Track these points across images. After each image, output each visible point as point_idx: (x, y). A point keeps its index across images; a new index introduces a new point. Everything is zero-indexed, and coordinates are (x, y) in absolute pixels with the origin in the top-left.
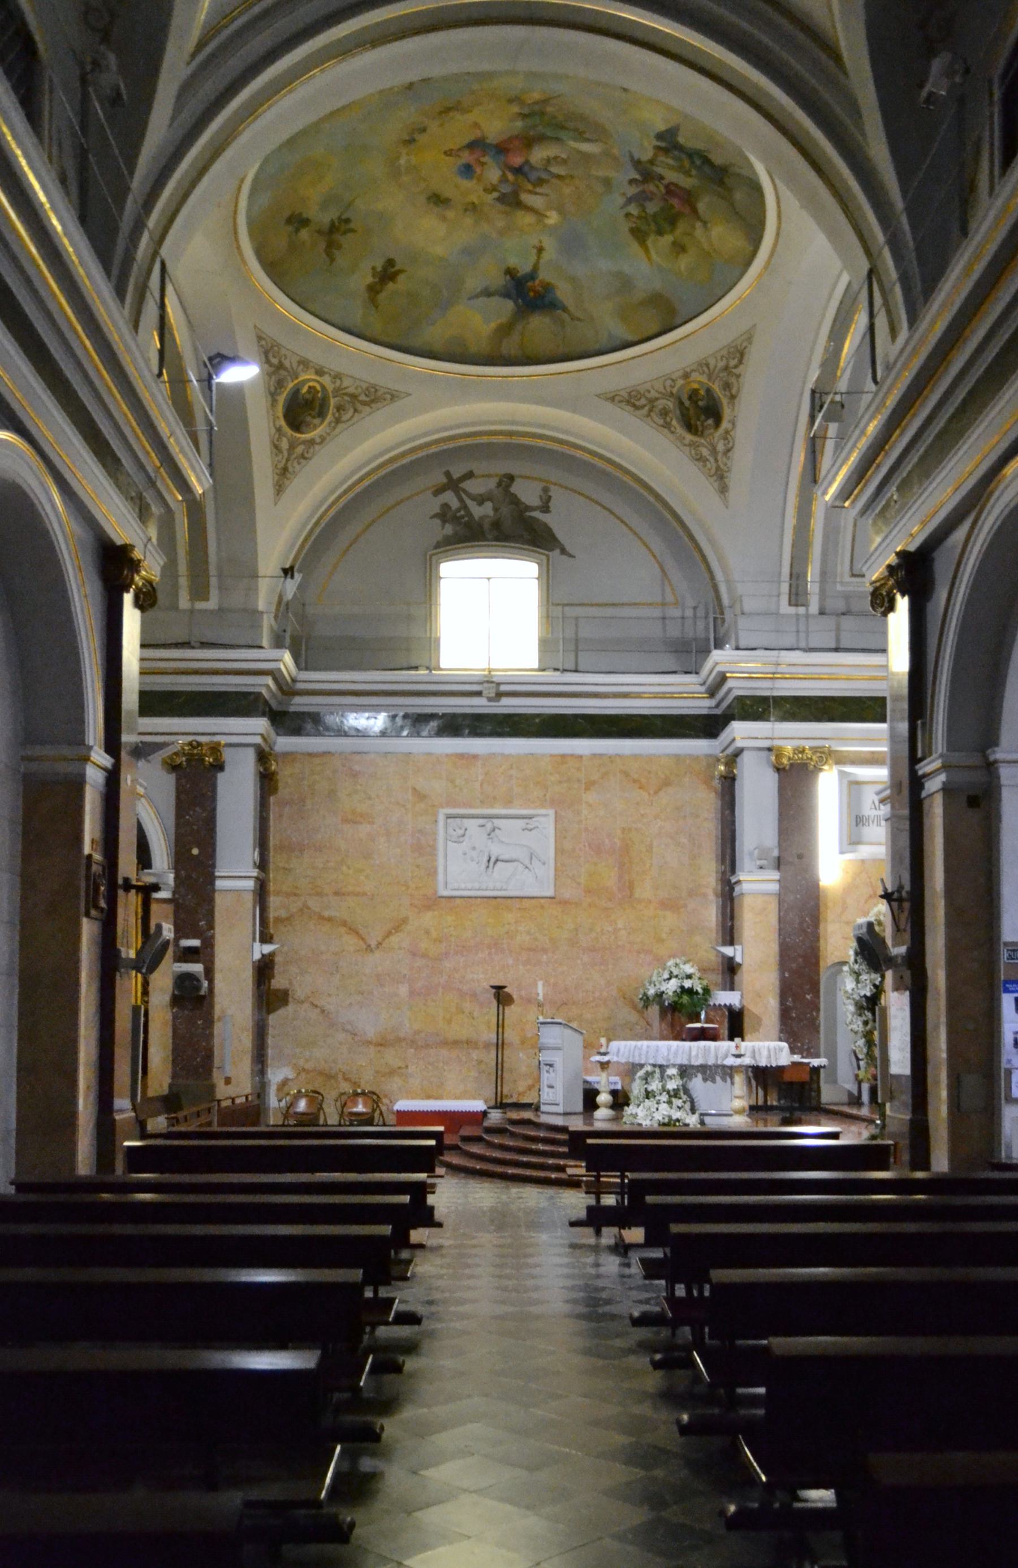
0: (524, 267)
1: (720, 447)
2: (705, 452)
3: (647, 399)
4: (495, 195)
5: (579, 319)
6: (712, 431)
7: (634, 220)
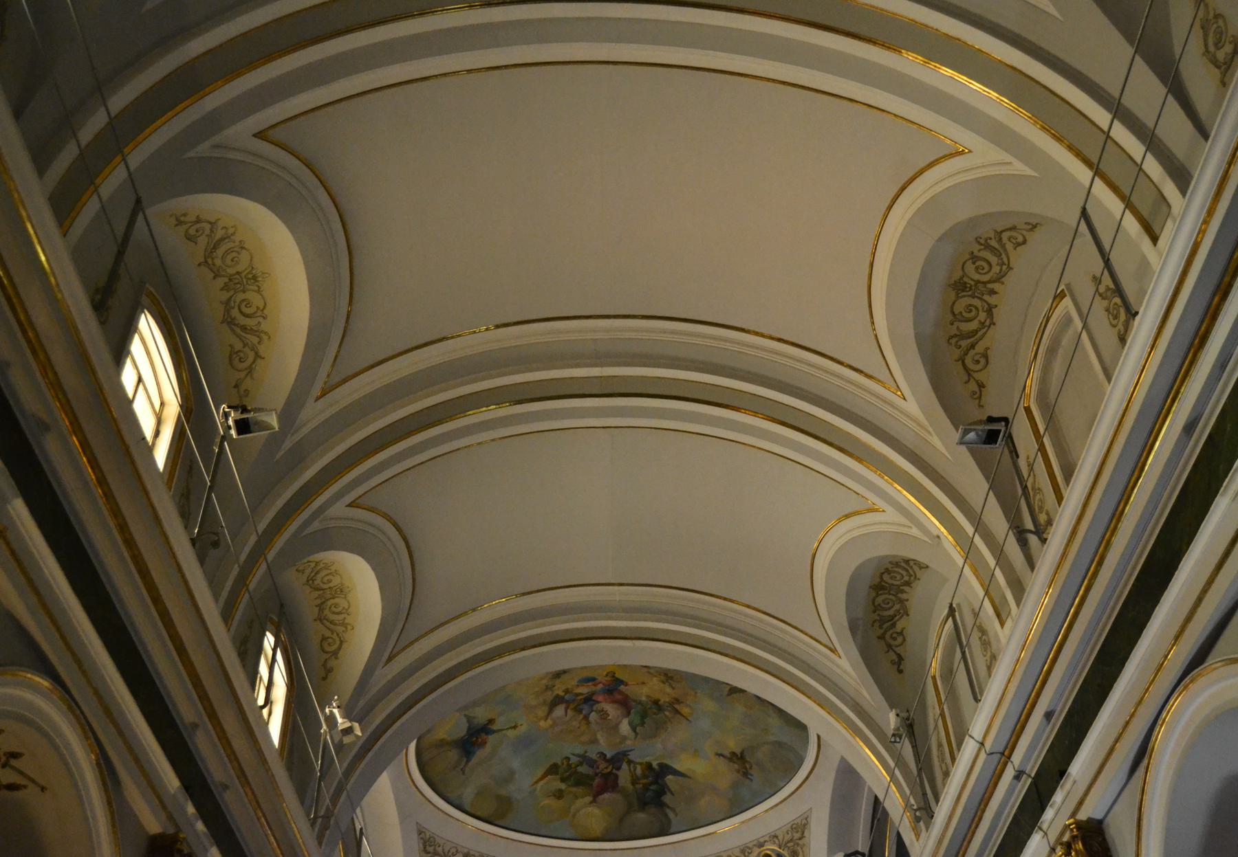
3: (435, 849)
4: (562, 694)
5: (464, 773)
7: (565, 763)
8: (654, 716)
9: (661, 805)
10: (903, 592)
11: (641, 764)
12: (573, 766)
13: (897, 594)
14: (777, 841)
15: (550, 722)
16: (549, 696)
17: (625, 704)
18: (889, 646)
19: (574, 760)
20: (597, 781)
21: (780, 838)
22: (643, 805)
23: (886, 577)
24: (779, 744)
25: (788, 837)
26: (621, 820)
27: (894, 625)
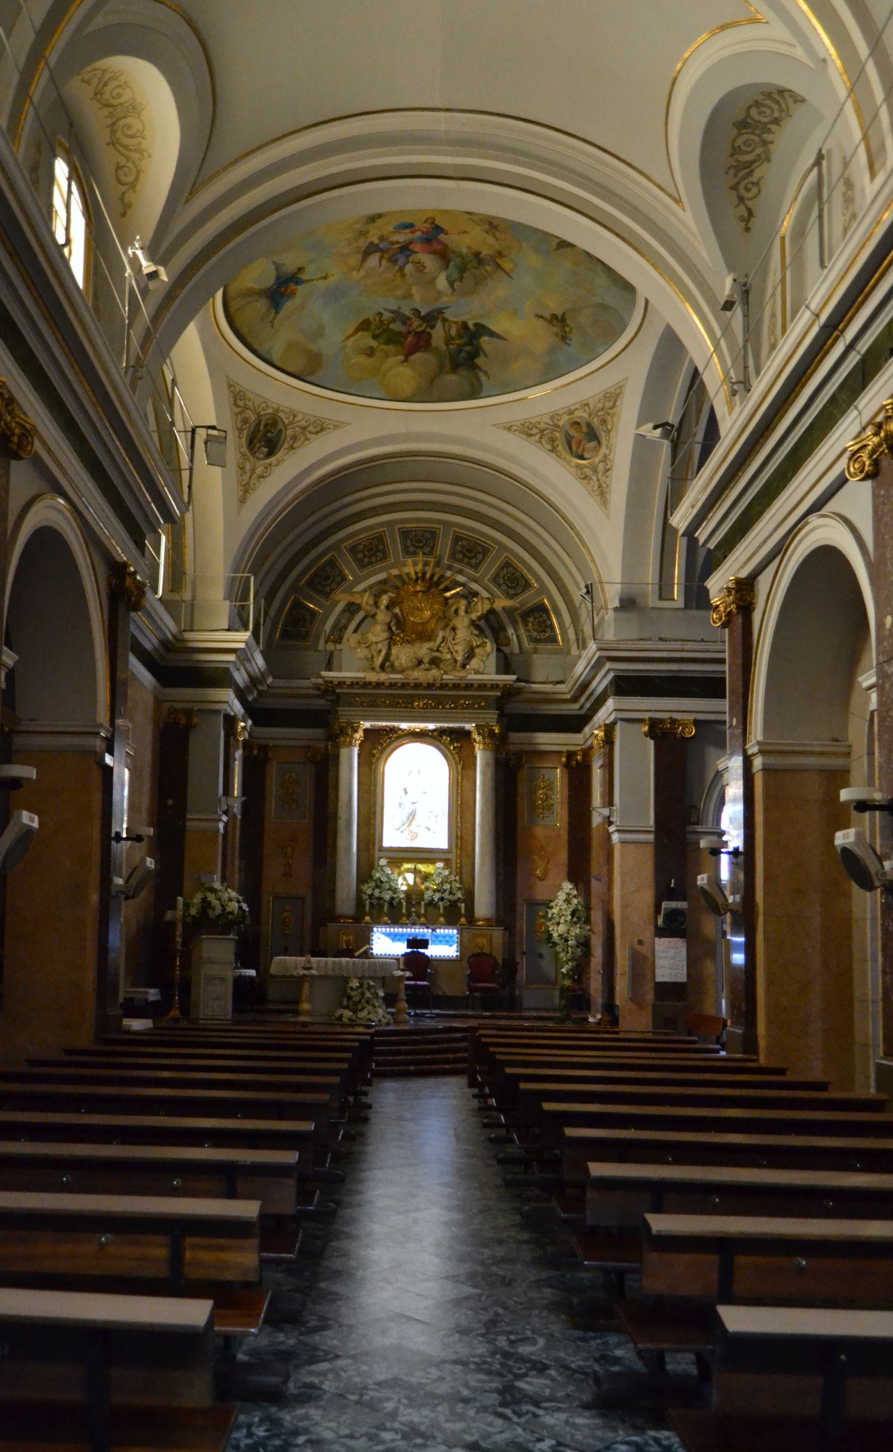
0: (304, 276)
1: (259, 471)
2: (248, 467)
3: (245, 404)
4: (376, 241)
5: (272, 326)
6: (261, 456)
7: (377, 319)
8: (474, 270)
9: (474, 368)
10: (769, 131)
11: (455, 323)
12: (386, 322)
13: (763, 133)
14: (588, 410)
15: (362, 273)
16: (363, 243)
17: (444, 255)
18: (741, 199)
19: (387, 316)
20: (410, 339)
21: (592, 407)
22: (455, 367)
23: (754, 112)
24: (604, 307)
25: (600, 406)
26: (432, 381)
27: (750, 173)
